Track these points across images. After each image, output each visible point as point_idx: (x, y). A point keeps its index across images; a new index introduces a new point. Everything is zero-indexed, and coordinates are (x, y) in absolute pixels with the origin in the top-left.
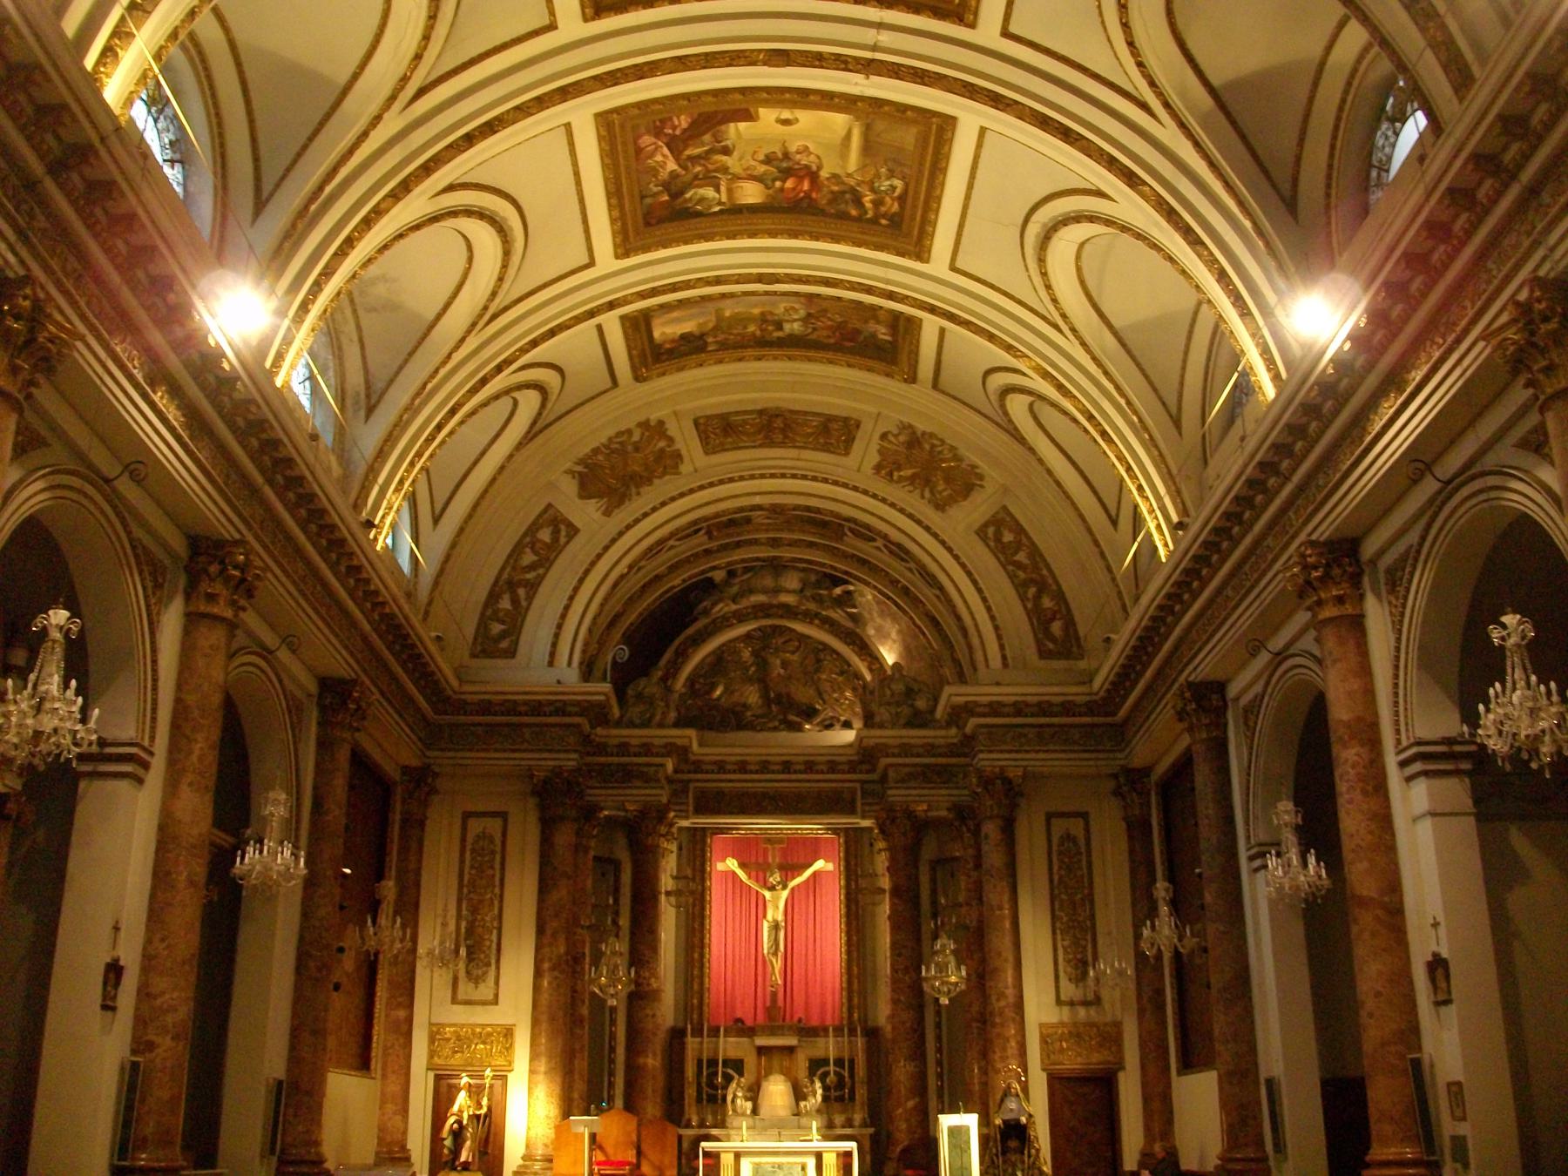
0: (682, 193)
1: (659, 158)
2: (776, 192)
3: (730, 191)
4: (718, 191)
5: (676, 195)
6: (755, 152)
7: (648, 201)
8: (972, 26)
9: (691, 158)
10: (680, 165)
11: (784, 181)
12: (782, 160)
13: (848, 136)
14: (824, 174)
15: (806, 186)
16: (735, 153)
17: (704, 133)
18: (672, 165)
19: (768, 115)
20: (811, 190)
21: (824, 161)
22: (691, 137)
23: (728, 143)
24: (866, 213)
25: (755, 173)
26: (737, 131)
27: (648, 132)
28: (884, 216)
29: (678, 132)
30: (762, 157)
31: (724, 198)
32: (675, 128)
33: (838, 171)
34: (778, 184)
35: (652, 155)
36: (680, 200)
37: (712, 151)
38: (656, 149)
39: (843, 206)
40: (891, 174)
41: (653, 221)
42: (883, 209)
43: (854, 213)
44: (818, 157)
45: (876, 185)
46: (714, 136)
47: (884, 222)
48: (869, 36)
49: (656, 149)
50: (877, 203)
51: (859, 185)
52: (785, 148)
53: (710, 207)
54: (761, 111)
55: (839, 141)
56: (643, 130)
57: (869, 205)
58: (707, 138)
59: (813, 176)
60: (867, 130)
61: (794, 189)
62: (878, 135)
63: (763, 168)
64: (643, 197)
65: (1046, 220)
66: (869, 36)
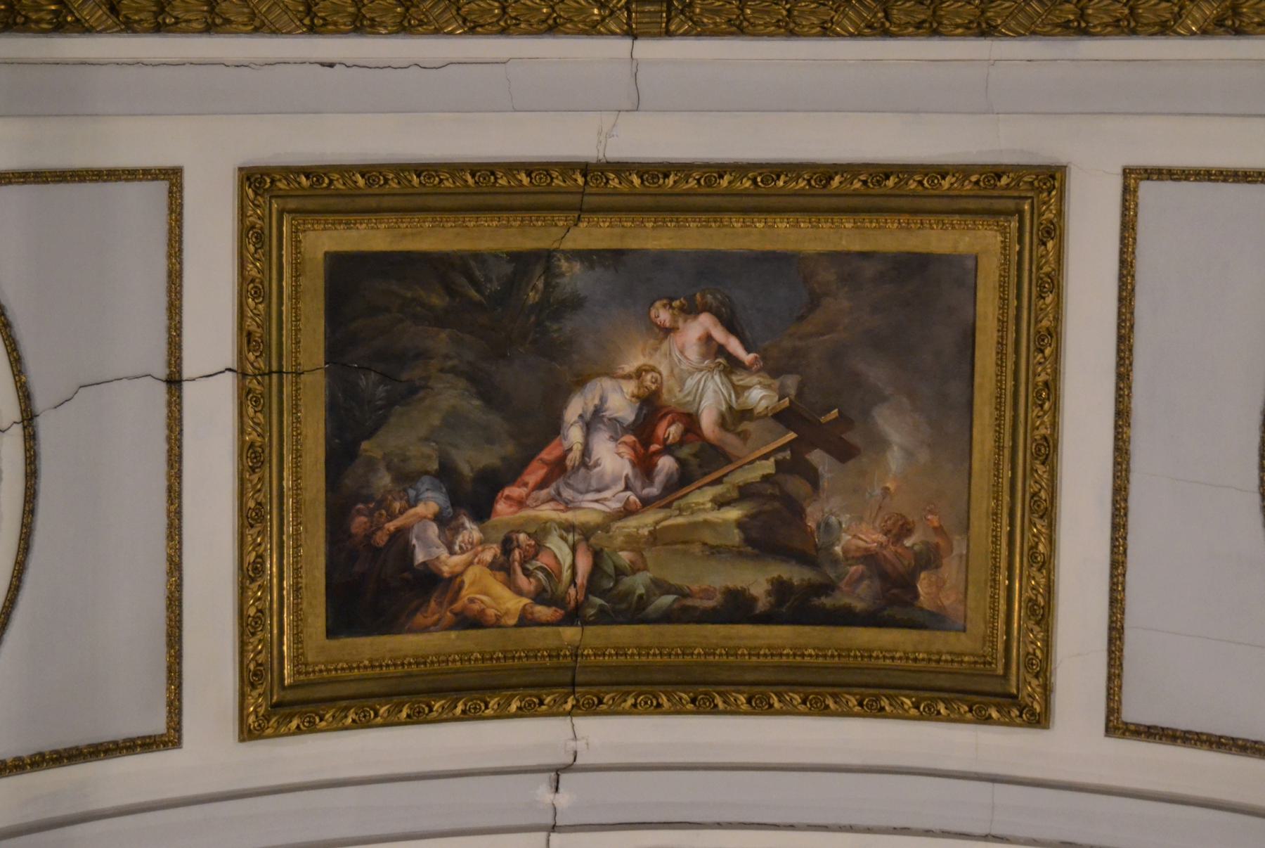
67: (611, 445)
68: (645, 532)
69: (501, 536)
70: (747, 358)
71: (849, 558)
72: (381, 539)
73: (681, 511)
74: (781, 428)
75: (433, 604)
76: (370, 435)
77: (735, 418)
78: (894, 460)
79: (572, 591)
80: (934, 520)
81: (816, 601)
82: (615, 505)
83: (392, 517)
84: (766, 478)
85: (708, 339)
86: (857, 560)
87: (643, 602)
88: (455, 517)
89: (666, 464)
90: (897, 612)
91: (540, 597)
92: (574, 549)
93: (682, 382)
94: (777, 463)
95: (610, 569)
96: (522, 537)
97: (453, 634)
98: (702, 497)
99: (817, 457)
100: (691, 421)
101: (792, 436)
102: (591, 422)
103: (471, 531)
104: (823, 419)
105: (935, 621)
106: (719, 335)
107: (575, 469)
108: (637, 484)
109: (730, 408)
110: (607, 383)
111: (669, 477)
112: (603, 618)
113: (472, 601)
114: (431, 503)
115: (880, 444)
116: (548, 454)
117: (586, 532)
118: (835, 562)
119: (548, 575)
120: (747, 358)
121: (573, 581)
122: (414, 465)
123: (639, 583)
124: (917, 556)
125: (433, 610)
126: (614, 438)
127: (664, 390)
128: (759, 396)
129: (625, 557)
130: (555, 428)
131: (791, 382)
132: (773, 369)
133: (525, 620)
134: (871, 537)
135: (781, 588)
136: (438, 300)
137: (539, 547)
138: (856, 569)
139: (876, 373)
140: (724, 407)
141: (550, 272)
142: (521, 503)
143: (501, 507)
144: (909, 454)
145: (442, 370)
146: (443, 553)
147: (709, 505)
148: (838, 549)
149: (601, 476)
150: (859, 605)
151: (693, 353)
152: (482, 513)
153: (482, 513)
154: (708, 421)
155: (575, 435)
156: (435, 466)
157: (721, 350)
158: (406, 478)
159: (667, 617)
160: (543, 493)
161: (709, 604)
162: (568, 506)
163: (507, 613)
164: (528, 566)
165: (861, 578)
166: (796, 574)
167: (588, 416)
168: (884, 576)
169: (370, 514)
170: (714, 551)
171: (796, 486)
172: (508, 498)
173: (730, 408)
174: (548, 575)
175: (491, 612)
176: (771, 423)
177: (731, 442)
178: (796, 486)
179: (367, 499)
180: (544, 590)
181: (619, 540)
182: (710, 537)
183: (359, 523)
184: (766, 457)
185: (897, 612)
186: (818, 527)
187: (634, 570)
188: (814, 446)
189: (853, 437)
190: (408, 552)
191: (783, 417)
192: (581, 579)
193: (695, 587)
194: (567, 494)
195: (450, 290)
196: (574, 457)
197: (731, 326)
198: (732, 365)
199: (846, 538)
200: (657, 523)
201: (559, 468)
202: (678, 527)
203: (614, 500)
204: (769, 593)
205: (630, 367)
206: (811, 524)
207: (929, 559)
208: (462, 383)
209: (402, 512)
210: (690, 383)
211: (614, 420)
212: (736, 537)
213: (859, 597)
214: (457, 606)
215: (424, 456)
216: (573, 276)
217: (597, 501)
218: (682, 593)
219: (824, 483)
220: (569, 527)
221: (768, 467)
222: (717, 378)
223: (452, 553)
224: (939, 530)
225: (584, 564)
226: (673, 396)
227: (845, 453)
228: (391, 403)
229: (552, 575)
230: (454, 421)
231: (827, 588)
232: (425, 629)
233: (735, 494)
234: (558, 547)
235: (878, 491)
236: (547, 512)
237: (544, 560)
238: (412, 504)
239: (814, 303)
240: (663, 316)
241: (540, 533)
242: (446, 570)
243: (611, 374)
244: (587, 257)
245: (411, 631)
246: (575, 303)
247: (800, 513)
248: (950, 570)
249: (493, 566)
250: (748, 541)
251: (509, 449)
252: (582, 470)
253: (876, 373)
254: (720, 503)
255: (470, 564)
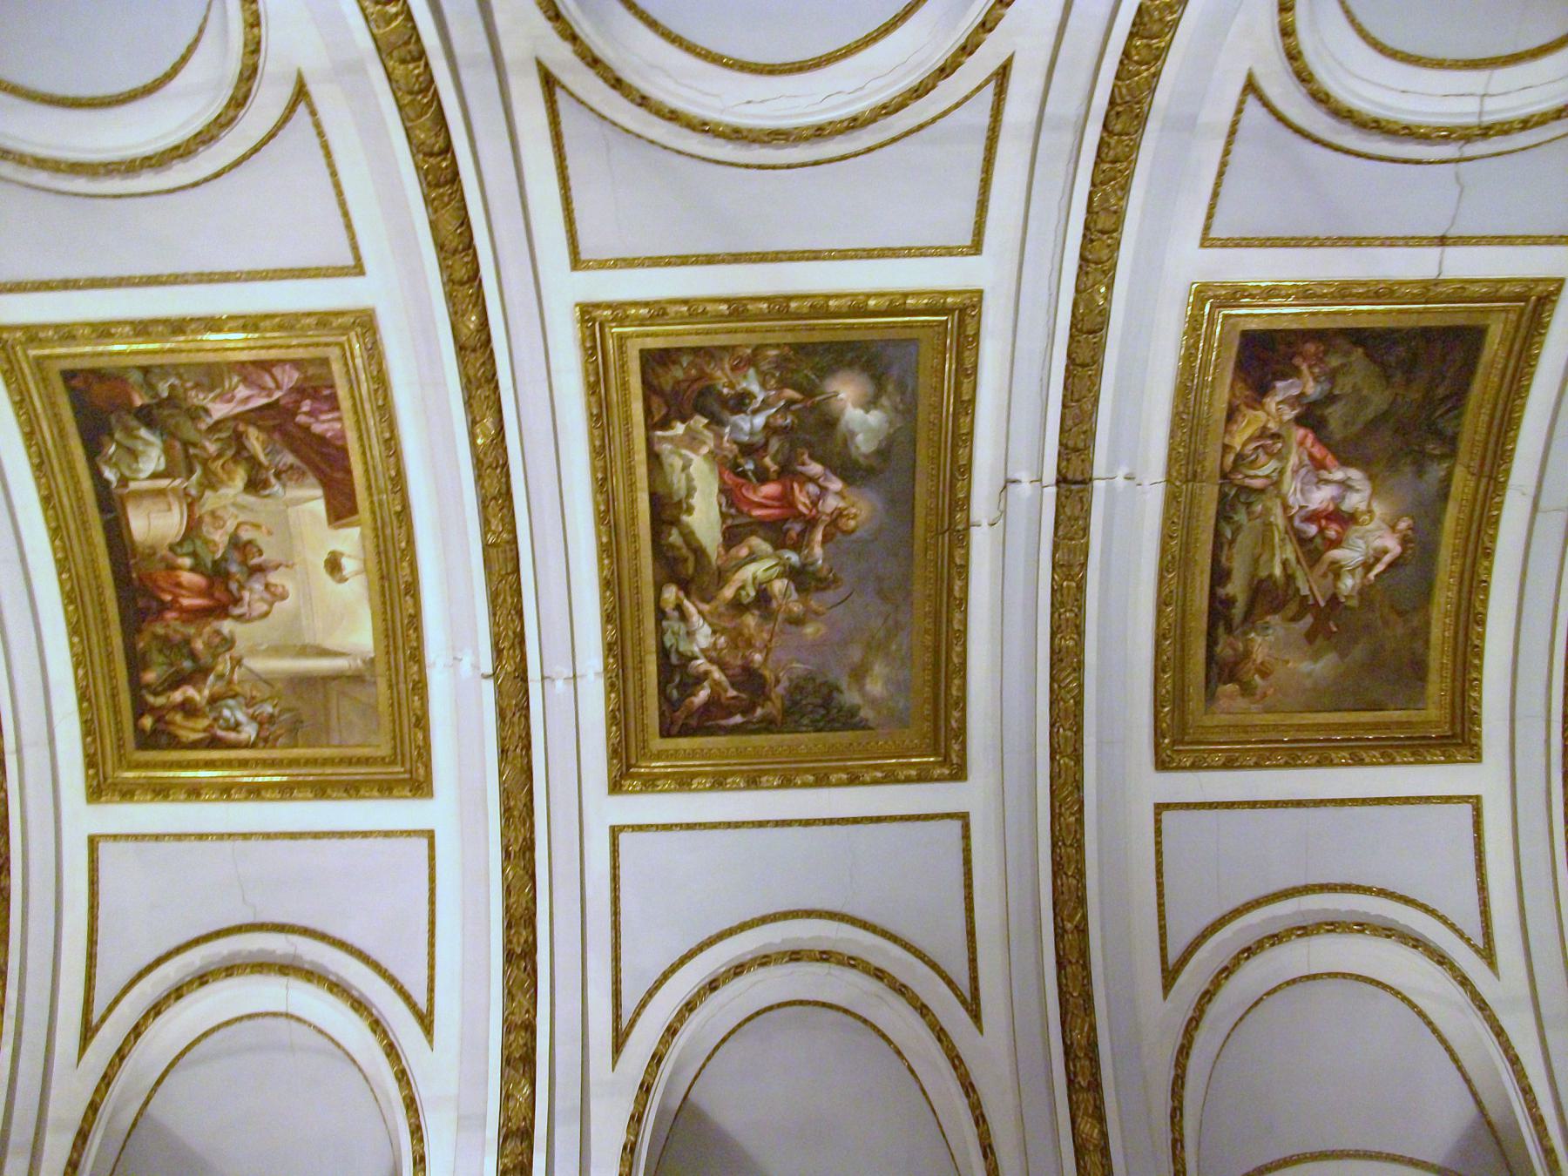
0: (150, 424)
1: (242, 392)
2: (163, 559)
3: (160, 493)
4: (155, 476)
5: (147, 417)
6: (257, 526)
7: (135, 377)
8: (615, 787)
9: (239, 438)
10: (218, 423)
11: (192, 569)
12: (244, 563)
13: (323, 653)
14: (227, 626)
15: (186, 602)
16: (250, 499)
17: (296, 452)
18: (220, 410)
19: (350, 541)
20: (183, 610)
21: (257, 626)
22: (285, 434)
23: (276, 487)
24: (156, 694)
25: (206, 529)
26: (310, 502)
27: (306, 379)
28: (159, 720)
29: (301, 419)
30: (245, 535)
31: (133, 485)
32: (310, 414)
33: (240, 647)
34: (187, 562)
35: (246, 380)
36: (133, 423)
37: (253, 464)
38: (262, 388)
39: (158, 658)
40: (262, 722)
41: (74, 383)
42: (178, 718)
43: (150, 676)
44: (265, 615)
45: (231, 702)
46: (291, 467)
47: (147, 722)
48: (561, 669)
49: (262, 388)
50: (188, 709)
51: (220, 677)
52: (277, 567)
53: (116, 466)
54: (355, 532)
55: (308, 639)
56: (311, 371)
57: (177, 696)
58: (289, 459)
59: (220, 610)
60: (356, 678)
61: (179, 585)
62: (343, 693)
63: (220, 538)
64: (146, 370)
65: (299, 952)
66: (561, 669)
67: (1329, 497)
68: (1272, 519)
69: (1283, 432)
70: (1372, 575)
71: (1247, 642)
72: (1297, 361)
73: (1282, 540)
74: (1328, 595)
75: (1247, 393)
76: (1367, 355)
77: (1336, 570)
78: (1305, 666)
79: (1240, 476)
80: (1270, 691)
81: (1221, 623)
82: (1291, 500)
83: (1310, 367)
84: (1298, 590)
85: (1385, 552)
86: (1246, 646)
87: (1228, 519)
88: (1300, 405)
89: (1312, 530)
90: (1215, 670)
91: (1240, 457)
92: (1267, 477)
93: (1361, 538)
94: (1306, 596)
95: (1252, 499)
96: (1280, 445)
97: (1225, 406)
98: (1290, 552)
99: (1309, 620)
100: (1336, 543)
101: (1322, 604)
102: (1345, 485)
103: (1289, 414)
104: (1332, 624)
105: (1210, 696)
106: (1387, 559)
107: (1317, 476)
108: (1303, 513)
109: (1341, 567)
110: (1367, 492)
111: (1305, 532)
112: (1223, 496)
113: (1244, 416)
114: (1312, 389)
115: (1316, 657)
116: (1330, 459)
117: (1277, 484)
118: (1245, 633)
119: (1253, 462)
120: (1372, 575)
121: (1247, 476)
122: (1340, 380)
123: (1241, 516)
124: (1249, 683)
125: (1243, 391)
126: (1333, 499)
127: (1357, 527)
128: (1348, 584)
129: (1258, 508)
130: (1345, 463)
131: (1354, 603)
132: (1364, 592)
133: (1226, 448)
134: (1260, 653)
135: (1229, 602)
136: (1441, 392)
137: (1271, 455)
138: (1240, 646)
139: (1358, 652)
140: (1343, 563)
141: (1443, 457)
142: (1301, 443)
143: (1300, 432)
144: (1309, 675)
145: (1397, 394)
146: (1279, 398)
147: (1284, 556)
148: (1253, 635)
149: (1310, 491)
150: (1218, 649)
151: (1378, 543)
152: (1299, 421)
153: (1299, 421)
154: (1335, 554)
155: (1338, 475)
156: (1337, 392)
157: (1377, 560)
158: (1332, 376)
159: (1218, 534)
160: (1306, 458)
161: (1223, 559)
162: (1295, 472)
163: (1233, 437)
164: (1260, 450)
165: (1235, 650)
166: (1238, 611)
167: (1349, 483)
168: (1236, 664)
169: (1316, 354)
170: (1256, 561)
171: (1293, 608)
172: (1306, 436)
173: (1341, 567)
174: (1253, 462)
175: (1235, 427)
176: (1329, 593)
177: (1321, 568)
178: (1293, 608)
179: (1326, 353)
180: (1244, 460)
181: (1269, 504)
182: (1264, 558)
183: (1310, 348)
184: (1311, 589)
185: (1215, 670)
186: (1267, 623)
187: (1249, 514)
188: (1315, 618)
189: (1320, 641)
190: (1284, 377)
191: (1334, 600)
192: (1248, 481)
193: (1234, 551)
194: (1303, 471)
195: (1447, 398)
196: (1325, 474)
197: (1391, 565)
198: (1367, 567)
199: (1259, 639)
200: (1277, 526)
201: (1319, 465)
202: (1272, 539)
203: (1295, 500)
204: (1227, 595)
205: (1378, 508)
206: (1268, 618)
207: (1247, 690)
208: (1385, 407)
209: (1312, 373)
210: (1360, 543)
211: (1343, 498)
212: (1263, 574)
213: (1223, 650)
214: (1243, 408)
215: (1344, 385)
216: (1436, 471)
217: (1295, 489)
218: (1232, 542)
219: (1293, 625)
220: (1281, 472)
221: (1305, 591)
222: (1361, 558)
223: (1279, 403)
224: (1264, 695)
225: (1257, 483)
226: (1354, 532)
227: (1310, 636)
228: (1384, 366)
229: (1253, 464)
230: (1362, 402)
231: (1229, 629)
232: (1232, 387)
233: (1290, 572)
234: (1270, 467)
235: (1287, 657)
236: (1293, 460)
237: (1263, 457)
238: (1316, 379)
239: (1401, 614)
240: (1403, 525)
241: (1281, 456)
242: (1267, 400)
243: (1373, 495)
244: (1446, 482)
245: (1234, 380)
246: (1420, 471)
247: (1275, 610)
248: (1241, 703)
249: (1264, 428)
250: (1261, 581)
251: (1338, 436)
252: (1315, 480)
253: (1358, 652)
254: (1285, 563)
255: (1268, 414)
